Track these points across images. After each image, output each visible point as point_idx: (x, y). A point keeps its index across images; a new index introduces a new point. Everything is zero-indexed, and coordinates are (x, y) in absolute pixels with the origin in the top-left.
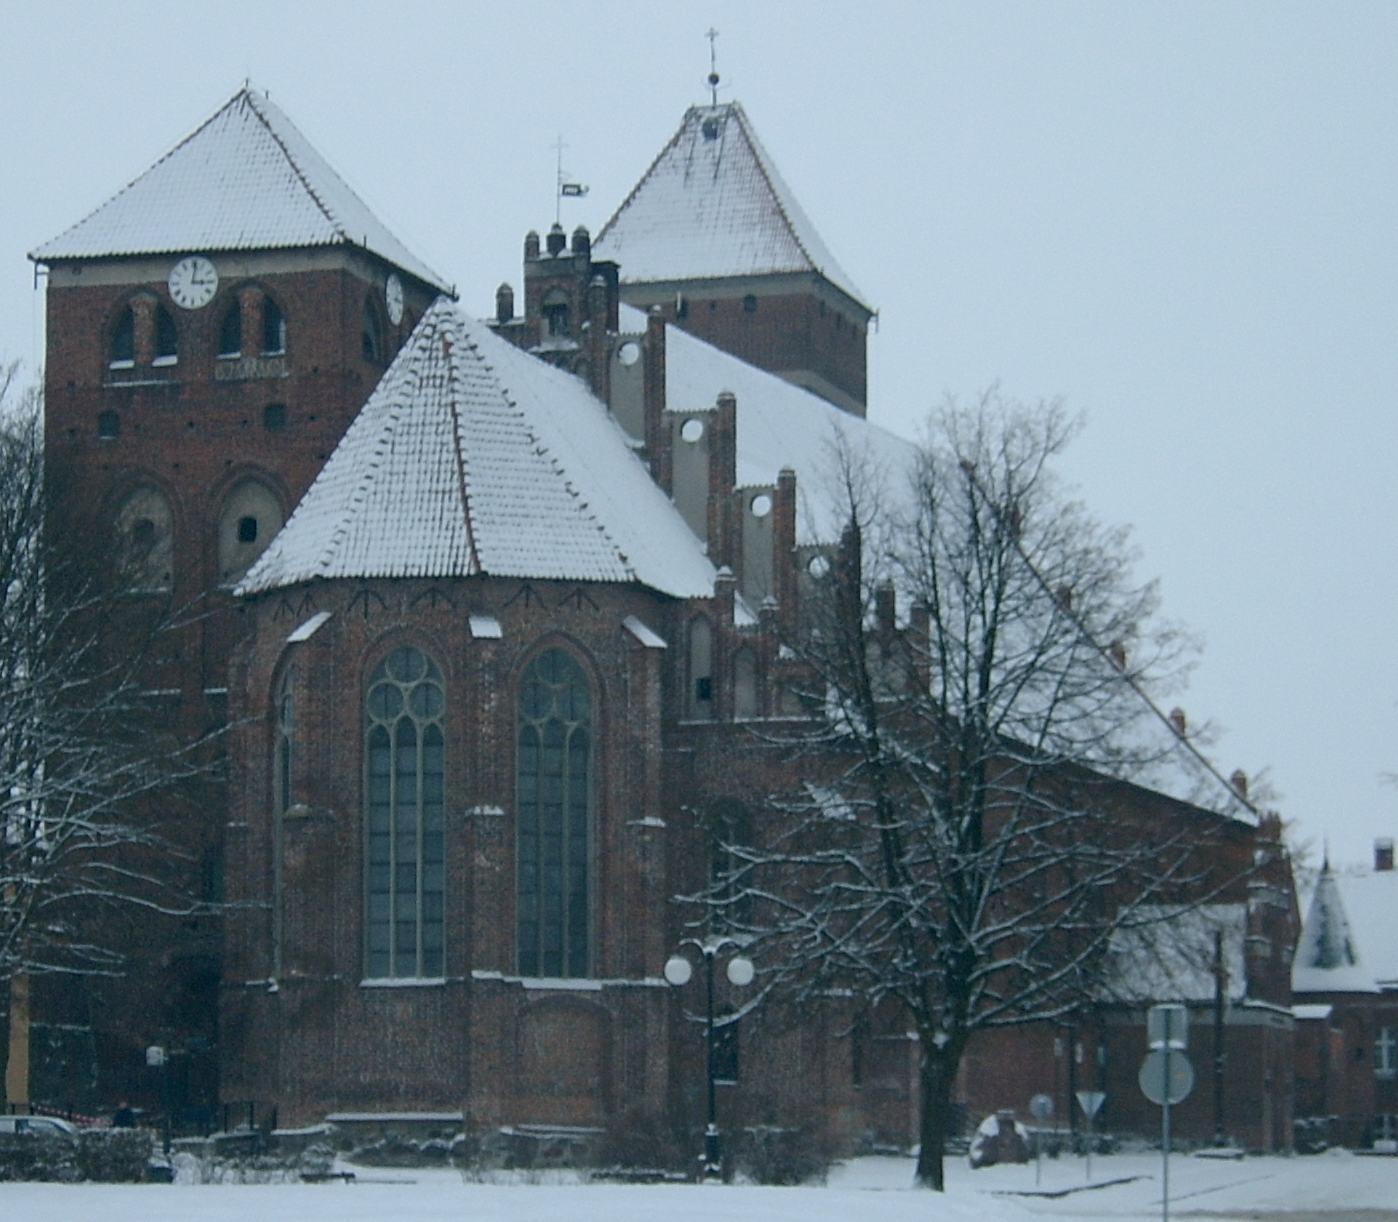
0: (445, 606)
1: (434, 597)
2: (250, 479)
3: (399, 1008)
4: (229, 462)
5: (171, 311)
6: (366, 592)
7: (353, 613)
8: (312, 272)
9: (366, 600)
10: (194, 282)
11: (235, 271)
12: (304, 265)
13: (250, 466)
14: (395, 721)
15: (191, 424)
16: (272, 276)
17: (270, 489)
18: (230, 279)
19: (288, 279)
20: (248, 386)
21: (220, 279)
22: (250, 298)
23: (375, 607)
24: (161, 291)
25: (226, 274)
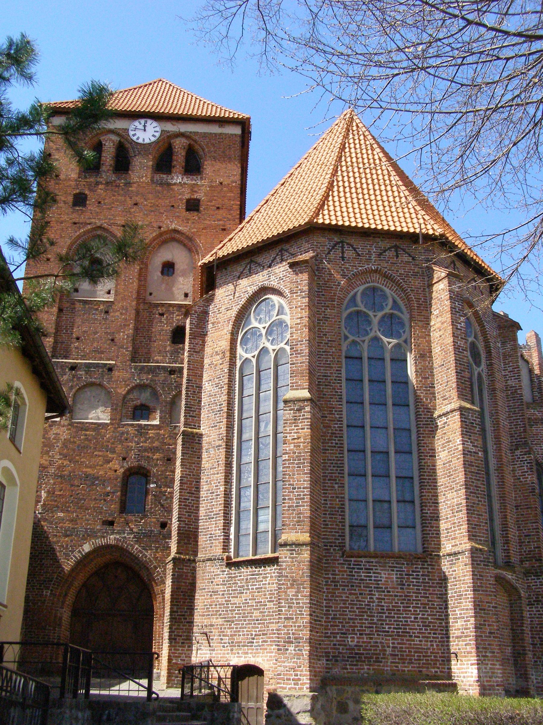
0: (406, 258)
1: (396, 251)
2: (173, 239)
3: (384, 575)
4: (160, 228)
5: (128, 146)
6: (342, 242)
7: (332, 255)
8: (221, 134)
9: (343, 247)
10: (145, 130)
11: (171, 127)
12: (214, 129)
13: (175, 231)
14: (367, 339)
15: (136, 204)
16: (196, 133)
17: (185, 245)
18: (168, 132)
19: (205, 135)
20: (176, 188)
21: (162, 131)
22: (179, 144)
23: (349, 253)
24: (123, 135)
25: (166, 129)
